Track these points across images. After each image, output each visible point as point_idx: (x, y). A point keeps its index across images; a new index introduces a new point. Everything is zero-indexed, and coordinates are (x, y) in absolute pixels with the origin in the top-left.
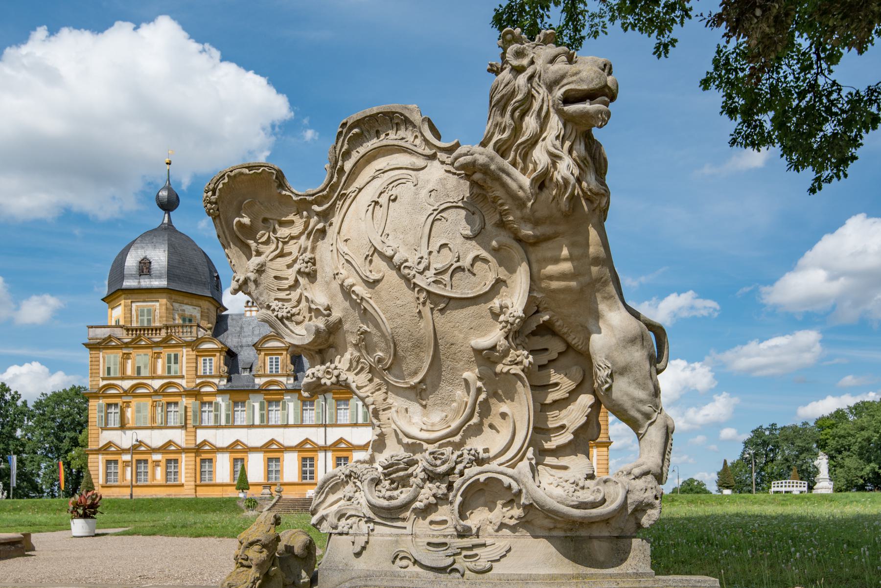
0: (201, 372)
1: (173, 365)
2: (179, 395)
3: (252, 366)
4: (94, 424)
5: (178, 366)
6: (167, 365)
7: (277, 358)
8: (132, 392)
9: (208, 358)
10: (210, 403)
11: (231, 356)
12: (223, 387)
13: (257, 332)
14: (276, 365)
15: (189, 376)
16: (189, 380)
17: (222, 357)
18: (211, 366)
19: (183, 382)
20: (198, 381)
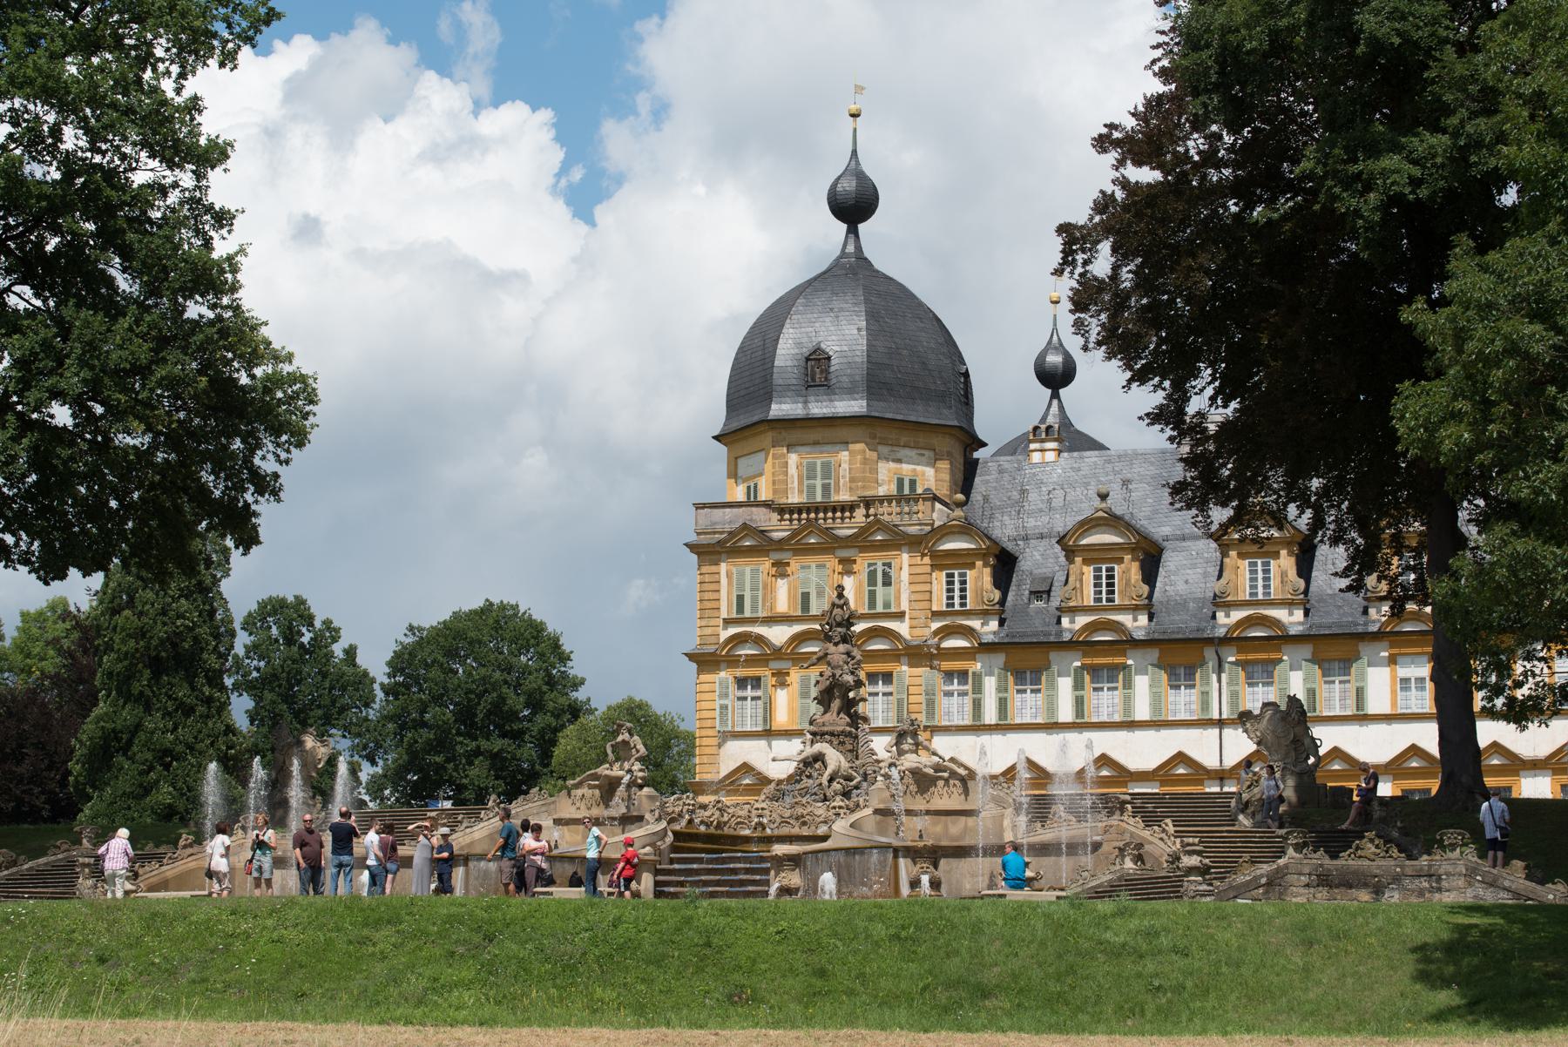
0: (939, 604)
1: (880, 589)
2: (893, 656)
3: (1051, 585)
4: (709, 723)
5: (892, 589)
6: (867, 589)
7: (1112, 569)
8: (792, 653)
9: (956, 573)
10: (963, 675)
11: (1004, 564)
12: (989, 638)
13: (1058, 502)
14: (1108, 585)
15: (915, 614)
16: (915, 622)
17: (987, 571)
18: (963, 590)
19: (902, 628)
20: (935, 625)
